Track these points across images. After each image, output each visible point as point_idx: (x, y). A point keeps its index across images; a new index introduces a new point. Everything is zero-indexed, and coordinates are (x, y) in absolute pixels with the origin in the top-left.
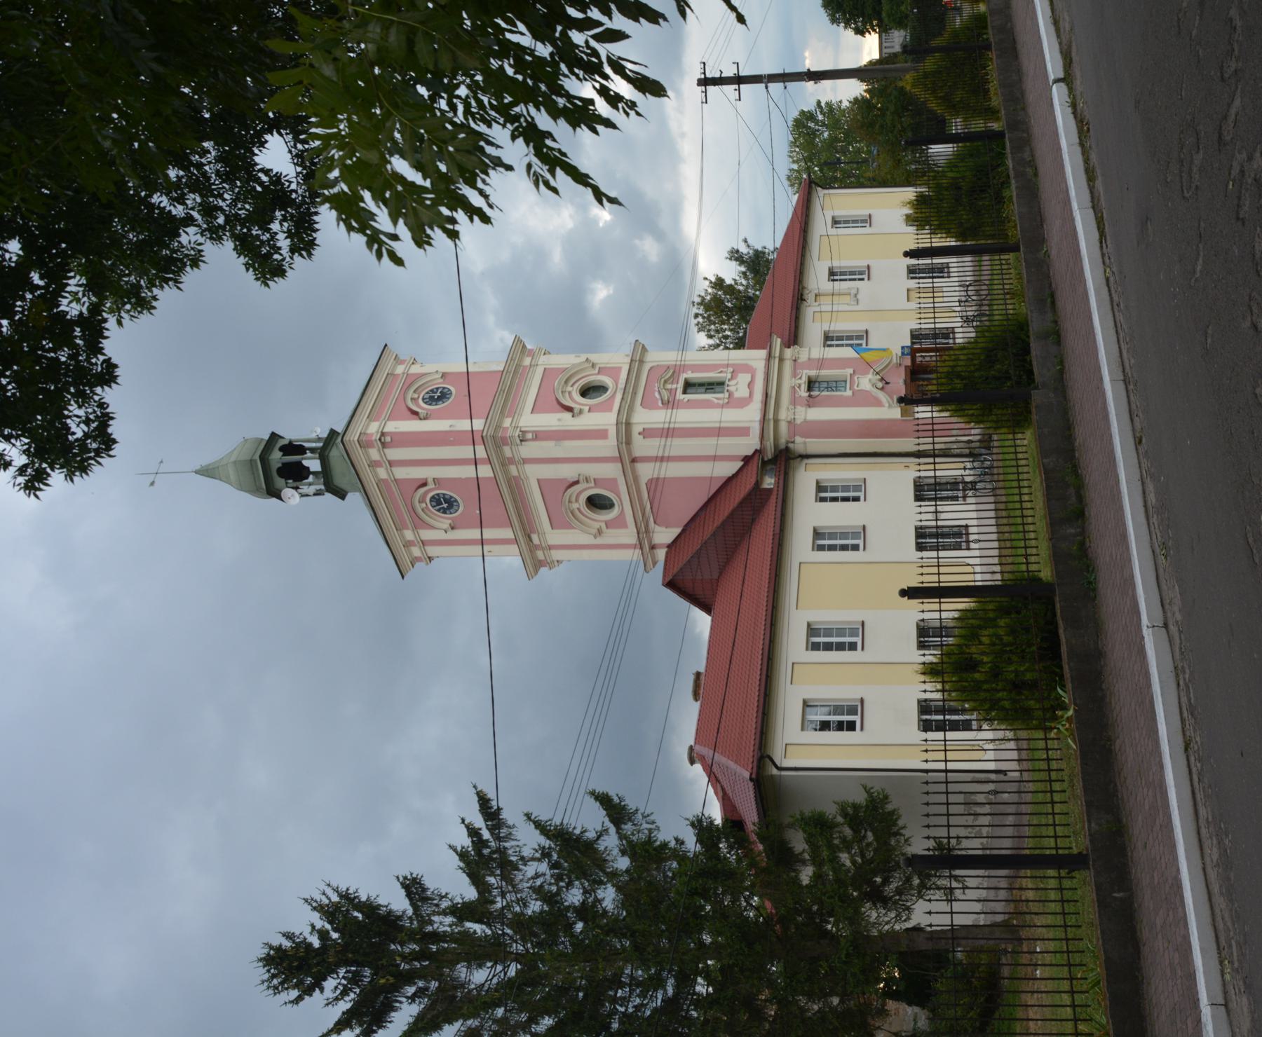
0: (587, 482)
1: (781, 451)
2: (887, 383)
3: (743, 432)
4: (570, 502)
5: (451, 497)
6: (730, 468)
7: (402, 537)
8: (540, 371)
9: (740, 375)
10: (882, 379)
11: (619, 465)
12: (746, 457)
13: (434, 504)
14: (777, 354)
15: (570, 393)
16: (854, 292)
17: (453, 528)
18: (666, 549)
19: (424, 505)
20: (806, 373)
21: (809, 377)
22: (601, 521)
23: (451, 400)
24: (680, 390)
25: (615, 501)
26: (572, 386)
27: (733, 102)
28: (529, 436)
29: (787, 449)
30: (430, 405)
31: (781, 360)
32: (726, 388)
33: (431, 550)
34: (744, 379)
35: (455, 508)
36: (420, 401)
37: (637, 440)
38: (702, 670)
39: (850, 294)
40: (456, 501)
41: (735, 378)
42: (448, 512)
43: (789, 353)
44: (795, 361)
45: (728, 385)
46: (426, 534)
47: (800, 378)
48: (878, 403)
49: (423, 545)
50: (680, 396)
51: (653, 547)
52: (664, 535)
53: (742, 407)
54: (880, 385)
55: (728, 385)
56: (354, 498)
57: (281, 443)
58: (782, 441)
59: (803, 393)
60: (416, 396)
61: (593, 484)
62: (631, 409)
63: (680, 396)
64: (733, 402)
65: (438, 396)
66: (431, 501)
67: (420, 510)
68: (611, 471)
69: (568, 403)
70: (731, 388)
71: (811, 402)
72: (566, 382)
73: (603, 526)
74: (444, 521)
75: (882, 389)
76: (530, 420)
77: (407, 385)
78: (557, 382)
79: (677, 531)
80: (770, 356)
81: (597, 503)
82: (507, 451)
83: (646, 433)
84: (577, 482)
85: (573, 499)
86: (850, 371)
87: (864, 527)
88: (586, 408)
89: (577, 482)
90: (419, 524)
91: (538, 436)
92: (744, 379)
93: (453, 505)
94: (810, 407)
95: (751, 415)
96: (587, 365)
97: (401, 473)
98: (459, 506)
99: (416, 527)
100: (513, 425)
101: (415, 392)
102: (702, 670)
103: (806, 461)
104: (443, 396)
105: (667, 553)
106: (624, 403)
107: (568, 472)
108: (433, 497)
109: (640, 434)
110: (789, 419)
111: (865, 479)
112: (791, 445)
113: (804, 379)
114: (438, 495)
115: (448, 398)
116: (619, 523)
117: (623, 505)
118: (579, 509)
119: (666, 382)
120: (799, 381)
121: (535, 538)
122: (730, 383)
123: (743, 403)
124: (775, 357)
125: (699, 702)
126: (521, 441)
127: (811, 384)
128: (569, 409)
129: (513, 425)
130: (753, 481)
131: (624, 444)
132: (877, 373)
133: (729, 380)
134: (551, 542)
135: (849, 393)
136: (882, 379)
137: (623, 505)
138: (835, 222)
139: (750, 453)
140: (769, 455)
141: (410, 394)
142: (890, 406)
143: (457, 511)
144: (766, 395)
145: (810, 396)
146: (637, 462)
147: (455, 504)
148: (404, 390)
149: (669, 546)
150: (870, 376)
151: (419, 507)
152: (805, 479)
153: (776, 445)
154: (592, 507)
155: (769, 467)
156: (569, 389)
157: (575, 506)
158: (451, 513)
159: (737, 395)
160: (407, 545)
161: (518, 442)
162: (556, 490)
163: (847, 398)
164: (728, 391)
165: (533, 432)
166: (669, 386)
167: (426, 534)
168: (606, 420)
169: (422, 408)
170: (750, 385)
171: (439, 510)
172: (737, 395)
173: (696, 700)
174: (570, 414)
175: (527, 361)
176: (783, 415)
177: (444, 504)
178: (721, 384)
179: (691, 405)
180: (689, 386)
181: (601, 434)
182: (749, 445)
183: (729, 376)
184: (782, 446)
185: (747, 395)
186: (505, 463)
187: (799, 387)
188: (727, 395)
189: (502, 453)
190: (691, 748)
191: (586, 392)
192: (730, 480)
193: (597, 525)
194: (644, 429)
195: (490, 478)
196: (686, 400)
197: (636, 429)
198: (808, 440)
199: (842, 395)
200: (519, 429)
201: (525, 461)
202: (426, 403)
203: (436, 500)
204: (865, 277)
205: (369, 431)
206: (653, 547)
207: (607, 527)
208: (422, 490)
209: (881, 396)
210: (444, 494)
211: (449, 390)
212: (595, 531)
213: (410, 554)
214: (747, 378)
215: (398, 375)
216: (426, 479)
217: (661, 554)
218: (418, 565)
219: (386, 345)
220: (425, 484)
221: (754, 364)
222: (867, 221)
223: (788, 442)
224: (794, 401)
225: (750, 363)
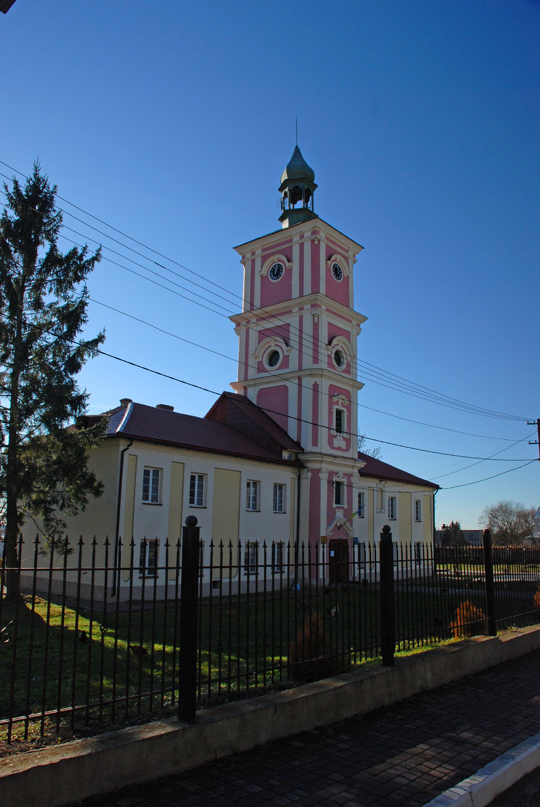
0: (287, 351)
2: (339, 528)
3: (315, 443)
5: (280, 276)
6: (293, 433)
9: (345, 443)
10: (341, 526)
12: (300, 444)
15: (338, 345)
16: (383, 510)
17: (261, 276)
19: (276, 261)
20: (345, 481)
21: (343, 482)
22: (262, 359)
23: (335, 279)
25: (275, 367)
26: (341, 346)
27: (528, 439)
30: (333, 268)
31: (353, 467)
35: (274, 278)
37: (312, 380)
38: (175, 411)
39: (382, 509)
40: (278, 278)
41: (343, 440)
42: (271, 274)
43: (356, 471)
45: (340, 435)
47: (343, 478)
48: (329, 523)
54: (338, 524)
55: (340, 435)
57: (311, 190)
58: (310, 465)
59: (335, 479)
60: (338, 261)
61: (285, 354)
62: (330, 378)
63: (335, 407)
64: (331, 439)
65: (337, 271)
66: (278, 264)
67: (274, 258)
69: (334, 342)
71: (330, 482)
73: (260, 360)
74: (266, 270)
75: (336, 525)
81: (274, 357)
85: (277, 343)
86: (346, 507)
88: (330, 353)
90: (264, 259)
92: (343, 445)
93: (275, 276)
95: (324, 447)
98: (275, 279)
100: (323, 311)
101: (340, 260)
102: (175, 411)
103: (296, 478)
105: (241, 395)
106: (333, 374)
108: (281, 266)
109: (316, 382)
110: (322, 470)
111: (286, 513)
112: (306, 470)
115: (336, 278)
116: (260, 369)
118: (271, 346)
120: (341, 477)
122: (341, 437)
125: (155, 407)
126: (313, 315)
127: (339, 484)
128: (330, 343)
129: (323, 311)
131: (310, 373)
133: (342, 436)
135: (335, 505)
139: (302, 446)
140: (301, 457)
143: (272, 278)
144: (336, 457)
145: (333, 482)
146: (299, 380)
147: (276, 277)
151: (275, 258)
153: (307, 461)
154: (271, 353)
156: (340, 345)
158: (270, 275)
159: (335, 440)
161: (313, 313)
165: (318, 322)
166: (340, 401)
169: (331, 264)
170: (339, 449)
171: (272, 268)
172: (335, 440)
173: (158, 406)
174: (327, 343)
176: (324, 466)
177: (276, 272)
181: (316, 359)
182: (307, 444)
185: (335, 446)
187: (338, 477)
190: (130, 401)
192: (285, 434)
194: (318, 385)
196: (333, 410)
197: (318, 380)
198: (309, 480)
200: (320, 314)
202: (334, 265)
204: (390, 518)
208: (285, 260)
211: (340, 279)
214: (344, 447)
216: (292, 262)
217: (242, 393)
219: (363, 248)
220: (289, 261)
221: (351, 451)
223: (308, 468)
225: (351, 448)
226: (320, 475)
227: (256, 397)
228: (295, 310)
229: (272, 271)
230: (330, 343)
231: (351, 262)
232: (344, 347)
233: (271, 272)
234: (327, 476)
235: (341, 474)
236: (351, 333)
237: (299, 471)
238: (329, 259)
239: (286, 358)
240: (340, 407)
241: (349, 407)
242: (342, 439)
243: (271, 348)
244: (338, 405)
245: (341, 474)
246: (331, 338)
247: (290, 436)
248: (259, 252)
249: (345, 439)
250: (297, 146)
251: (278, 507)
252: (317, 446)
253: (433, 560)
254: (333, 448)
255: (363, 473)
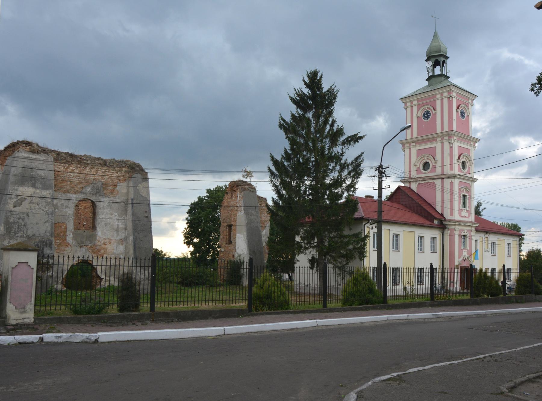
1: (445, 226)
2: (465, 261)
3: (452, 214)
4: (427, 157)
5: (429, 118)
6: (439, 209)
7: (415, 100)
8: (469, 148)
10: (466, 259)
11: (441, 174)
12: (443, 215)
13: (427, 112)
14: (474, 225)
15: (463, 158)
16: (488, 250)
17: (417, 117)
18: (409, 187)
19: (426, 108)
20: (468, 234)
21: (466, 235)
24: (463, 194)
28: (451, 145)
29: (446, 228)
31: (472, 226)
33: (409, 110)
34: (466, 214)
35: (425, 119)
36: (461, 109)
39: (487, 249)
40: (428, 119)
43: (473, 229)
44: (471, 231)
46: (415, 109)
48: (459, 258)
49: (411, 107)
50: (462, 193)
51: (410, 182)
52: (414, 187)
54: (464, 258)
56: (426, 83)
57: (445, 60)
58: (449, 227)
60: (463, 107)
64: (460, 210)
66: (428, 111)
68: (439, 171)
69: (461, 157)
70: (464, 210)
71: (460, 236)
72: (466, 157)
73: (418, 167)
74: (420, 114)
75: (463, 259)
76: (456, 145)
77: (466, 104)
79: (416, 191)
80: (473, 223)
81: (426, 166)
82: (446, 138)
83: (452, 183)
84: (435, 160)
86: (468, 249)
87: (424, 252)
89: (435, 160)
90: (419, 107)
91: (451, 148)
92: (466, 214)
94: (459, 236)
95: (457, 217)
96: (471, 163)
97: (438, 103)
99: (418, 105)
103: (441, 234)
104: (463, 116)
107: (438, 156)
108: (429, 112)
112: (447, 229)
113: (466, 234)
114: (430, 113)
117: (425, 174)
118: (424, 159)
119: (466, 189)
121: (414, 144)
123: (460, 215)
125: (364, 197)
126: (450, 143)
127: (465, 236)
130: (437, 217)
132: (468, 258)
134: (412, 149)
135: (462, 248)
136: (466, 259)
137: (425, 174)
138: (509, 244)
139: (444, 216)
140: (444, 222)
141: (464, 105)
142: (458, 261)
145: (462, 236)
148: (465, 103)
149: (410, 188)
150: (467, 255)
151: (426, 107)
152: (436, 233)
155: (440, 222)
157: (426, 158)
160: (412, 102)
162: (432, 152)
163: (461, 248)
165: (453, 146)
167: (415, 109)
168: (456, 170)
171: (424, 113)
172: (462, 212)
173: (366, 196)
174: (457, 158)
175: (472, 143)
176: (457, 227)
177: (427, 115)
178: (465, 207)
179: (460, 197)
180: (464, 196)
181: (451, 169)
182: (447, 216)
183: (467, 210)
184: (447, 227)
185: (462, 216)
186: (442, 137)
187: (464, 232)
188: (462, 208)
189: (445, 136)
191: (463, 163)
192: (434, 209)
193: (418, 165)
195: (436, 131)
197: (453, 180)
201: (443, 144)
203: (428, 113)
205: (453, 93)
206: (410, 182)
207: (417, 168)
209: (461, 259)
210: (430, 115)
212: (416, 164)
213: (408, 102)
214: (467, 216)
215: (468, 101)
216: (436, 110)
217: (407, 185)
218: (404, 104)
220: (434, 110)
221: (470, 218)
222: (509, 256)
223: (448, 228)
224: (460, 231)
226: (455, 232)
227: (416, 188)
228: (439, 139)
229: (424, 115)
230: (459, 158)
231: (470, 106)
232: (466, 158)
233: (423, 115)
234: (458, 232)
235: (466, 231)
237: (443, 230)
238: (458, 108)
239: (434, 167)
243: (424, 160)
244: (464, 192)
245: (466, 231)
246: (459, 154)
247: (438, 211)
248: (415, 102)
249: (468, 211)
250: (435, 31)
251: (433, 250)
252: (453, 216)
254: (462, 217)
255: (478, 230)
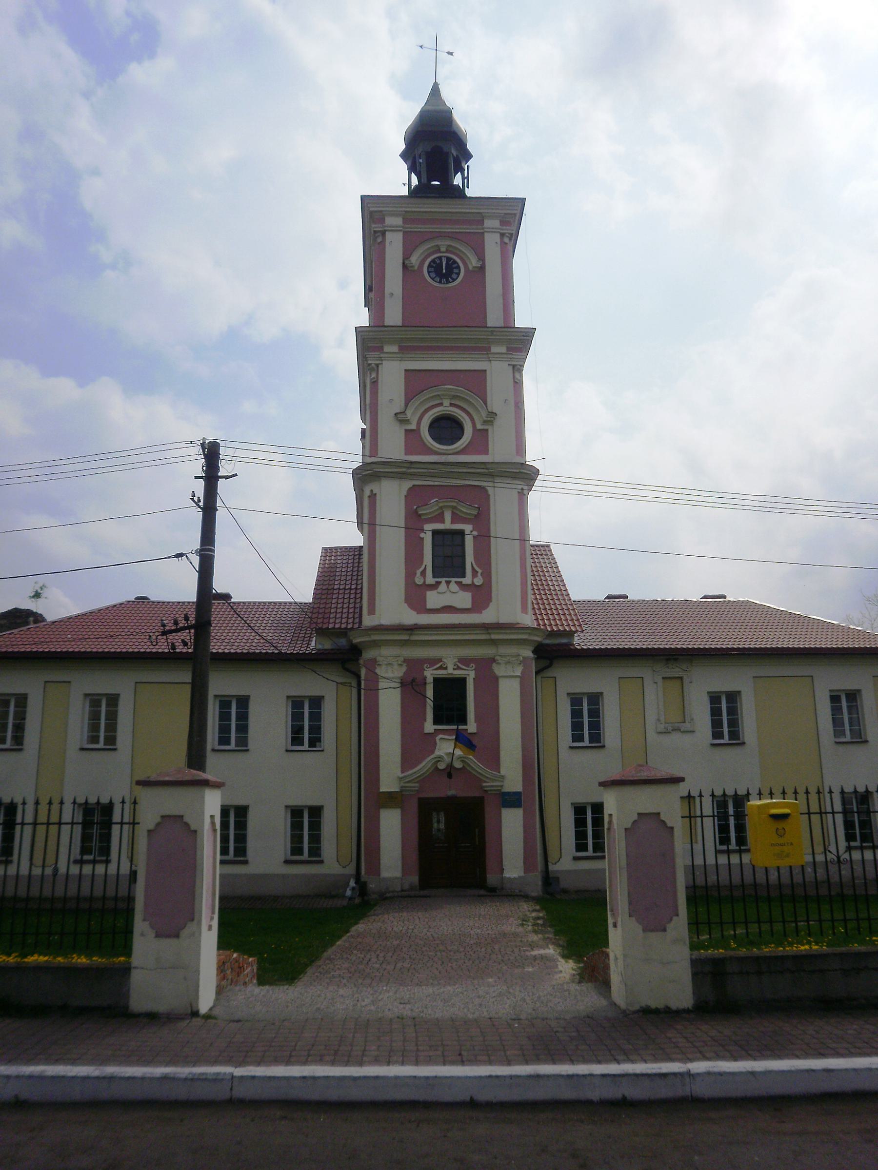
15: (441, 404)
26: (451, 405)
32: (443, 580)
45: (448, 583)
47: (459, 668)
53: (406, 602)
55: (448, 583)
62: (402, 476)
63: (429, 527)
70: (443, 587)
78: (451, 387)
88: (413, 426)
92: (464, 599)
96: (484, 414)
106: (408, 465)
124: (489, 634)
135: (429, 727)
156: (446, 403)
164: (439, 583)
170: (449, 609)
187: (441, 668)
199: (425, 720)
236: (488, 373)
240: (448, 524)
241: (481, 519)
242: (454, 587)
253: (716, 818)
